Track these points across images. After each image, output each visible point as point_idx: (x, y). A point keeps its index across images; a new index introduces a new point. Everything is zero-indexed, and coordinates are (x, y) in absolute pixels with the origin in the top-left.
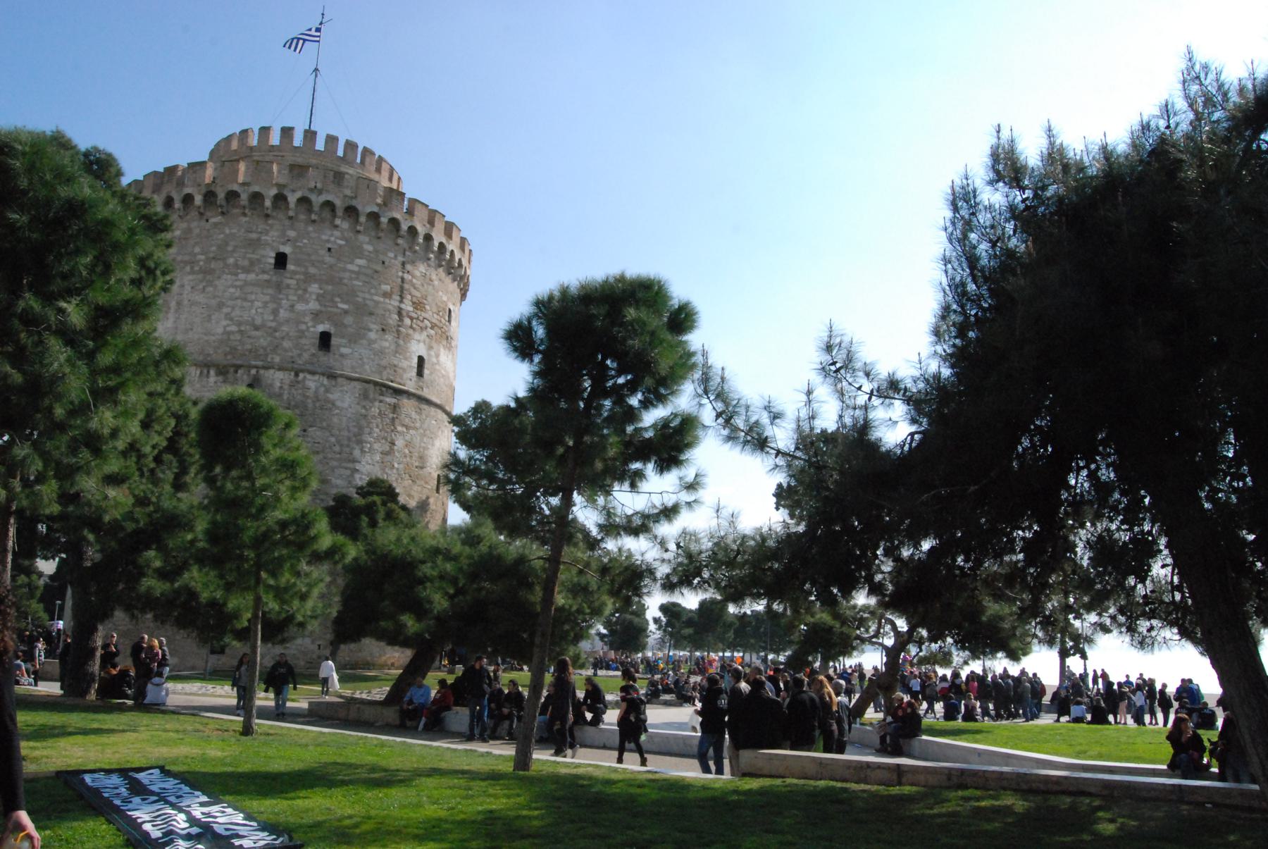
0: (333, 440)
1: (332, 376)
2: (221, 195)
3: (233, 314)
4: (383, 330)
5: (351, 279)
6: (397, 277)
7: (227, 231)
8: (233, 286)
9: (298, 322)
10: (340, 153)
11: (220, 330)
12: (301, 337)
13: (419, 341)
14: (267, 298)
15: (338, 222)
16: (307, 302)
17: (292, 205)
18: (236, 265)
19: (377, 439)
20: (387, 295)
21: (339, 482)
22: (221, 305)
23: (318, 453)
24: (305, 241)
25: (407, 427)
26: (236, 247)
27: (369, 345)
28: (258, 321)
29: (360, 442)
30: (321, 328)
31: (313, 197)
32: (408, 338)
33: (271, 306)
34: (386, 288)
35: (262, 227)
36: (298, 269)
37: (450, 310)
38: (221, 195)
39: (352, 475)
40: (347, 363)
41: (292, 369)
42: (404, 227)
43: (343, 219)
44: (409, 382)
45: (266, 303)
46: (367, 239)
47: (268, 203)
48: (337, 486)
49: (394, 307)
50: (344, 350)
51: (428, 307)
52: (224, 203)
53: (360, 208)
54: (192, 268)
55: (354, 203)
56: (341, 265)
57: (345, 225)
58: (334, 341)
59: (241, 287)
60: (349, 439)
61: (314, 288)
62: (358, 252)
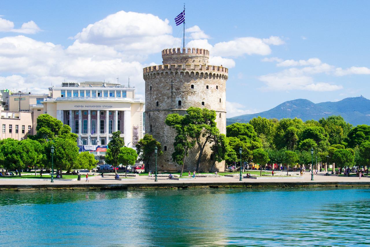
0: (160, 124)
1: (159, 111)
4: (168, 98)
5: (161, 88)
14: (150, 97)
15: (157, 77)
20: (168, 90)
23: (157, 128)
30: (157, 101)
31: (152, 73)
34: (168, 88)
40: (161, 107)
42: (169, 73)
43: (158, 76)
50: (161, 105)
51: (180, 88)
58: (159, 103)
61: (155, 93)
62: (161, 82)
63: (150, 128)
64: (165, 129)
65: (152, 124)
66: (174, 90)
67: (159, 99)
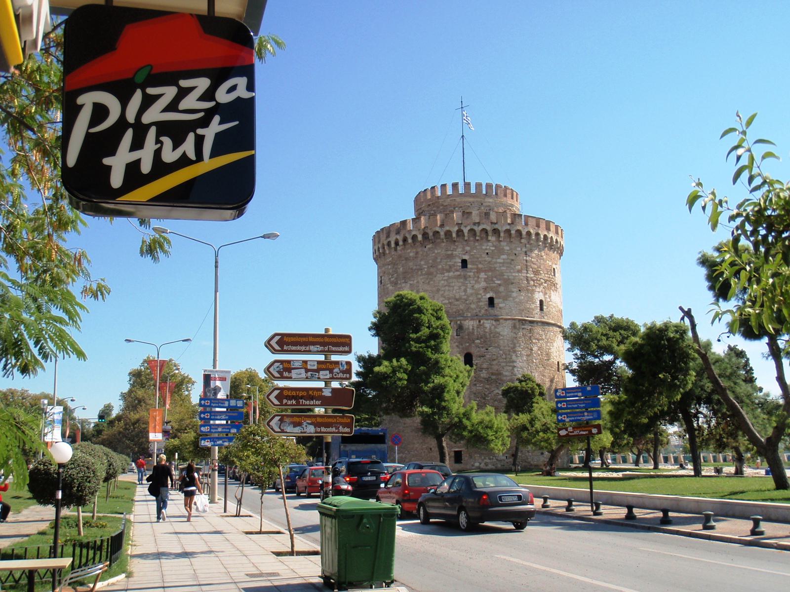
0: (501, 352)
1: (497, 320)
2: (431, 234)
3: (445, 295)
5: (500, 267)
6: (524, 260)
7: (436, 252)
8: (442, 280)
12: (479, 302)
13: (539, 292)
14: (460, 284)
15: (490, 238)
16: (479, 283)
17: (466, 234)
18: (443, 269)
21: (507, 373)
22: (438, 290)
23: (495, 360)
24: (475, 251)
25: (538, 340)
26: (441, 259)
27: (513, 300)
28: (457, 297)
29: (515, 352)
30: (488, 296)
31: (476, 228)
32: (533, 292)
33: (463, 288)
36: (473, 267)
37: (554, 269)
38: (431, 234)
39: (513, 369)
41: (477, 319)
42: (524, 233)
45: (460, 286)
46: (505, 244)
47: (454, 235)
48: (506, 376)
49: (524, 276)
50: (501, 305)
51: (541, 272)
52: (433, 238)
54: (421, 272)
55: (496, 226)
56: (494, 260)
58: (496, 301)
59: (447, 280)
60: (509, 351)
61: (482, 275)
62: (501, 252)
65: (474, 351)
67: (497, 292)
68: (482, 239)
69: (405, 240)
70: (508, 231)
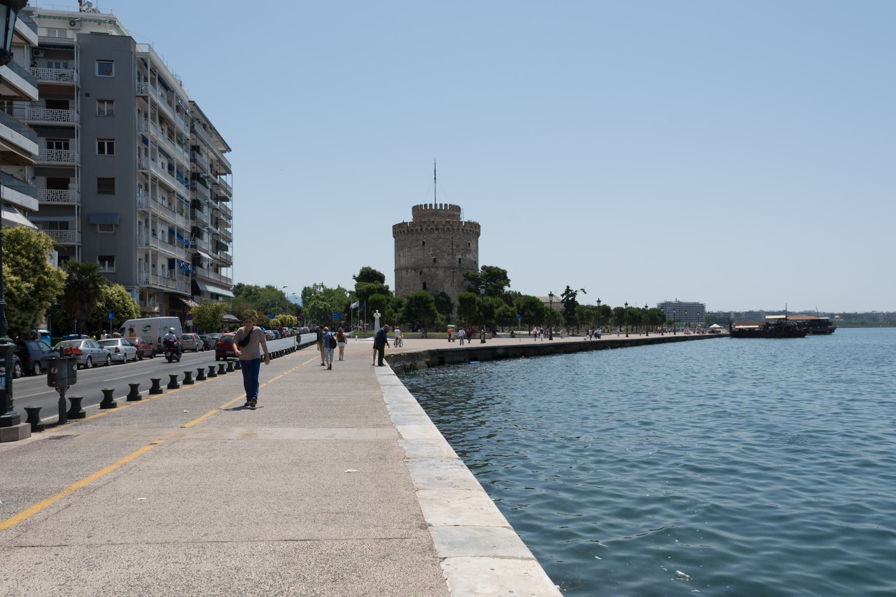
1: (437, 268)
2: (410, 230)
4: (448, 255)
9: (429, 257)
10: (438, 208)
11: (413, 261)
18: (415, 246)
19: (449, 280)
20: (448, 246)
22: (413, 256)
29: (445, 282)
30: (433, 258)
31: (428, 228)
32: (455, 255)
33: (423, 254)
34: (448, 244)
35: (419, 236)
38: (410, 230)
42: (451, 229)
44: (457, 265)
47: (419, 231)
50: (439, 262)
53: (439, 228)
57: (437, 232)
58: (437, 260)
61: (431, 249)
63: (422, 285)
64: (445, 287)
65: (427, 282)
66: (454, 247)
68: (431, 232)
69: (401, 232)
70: (443, 229)
